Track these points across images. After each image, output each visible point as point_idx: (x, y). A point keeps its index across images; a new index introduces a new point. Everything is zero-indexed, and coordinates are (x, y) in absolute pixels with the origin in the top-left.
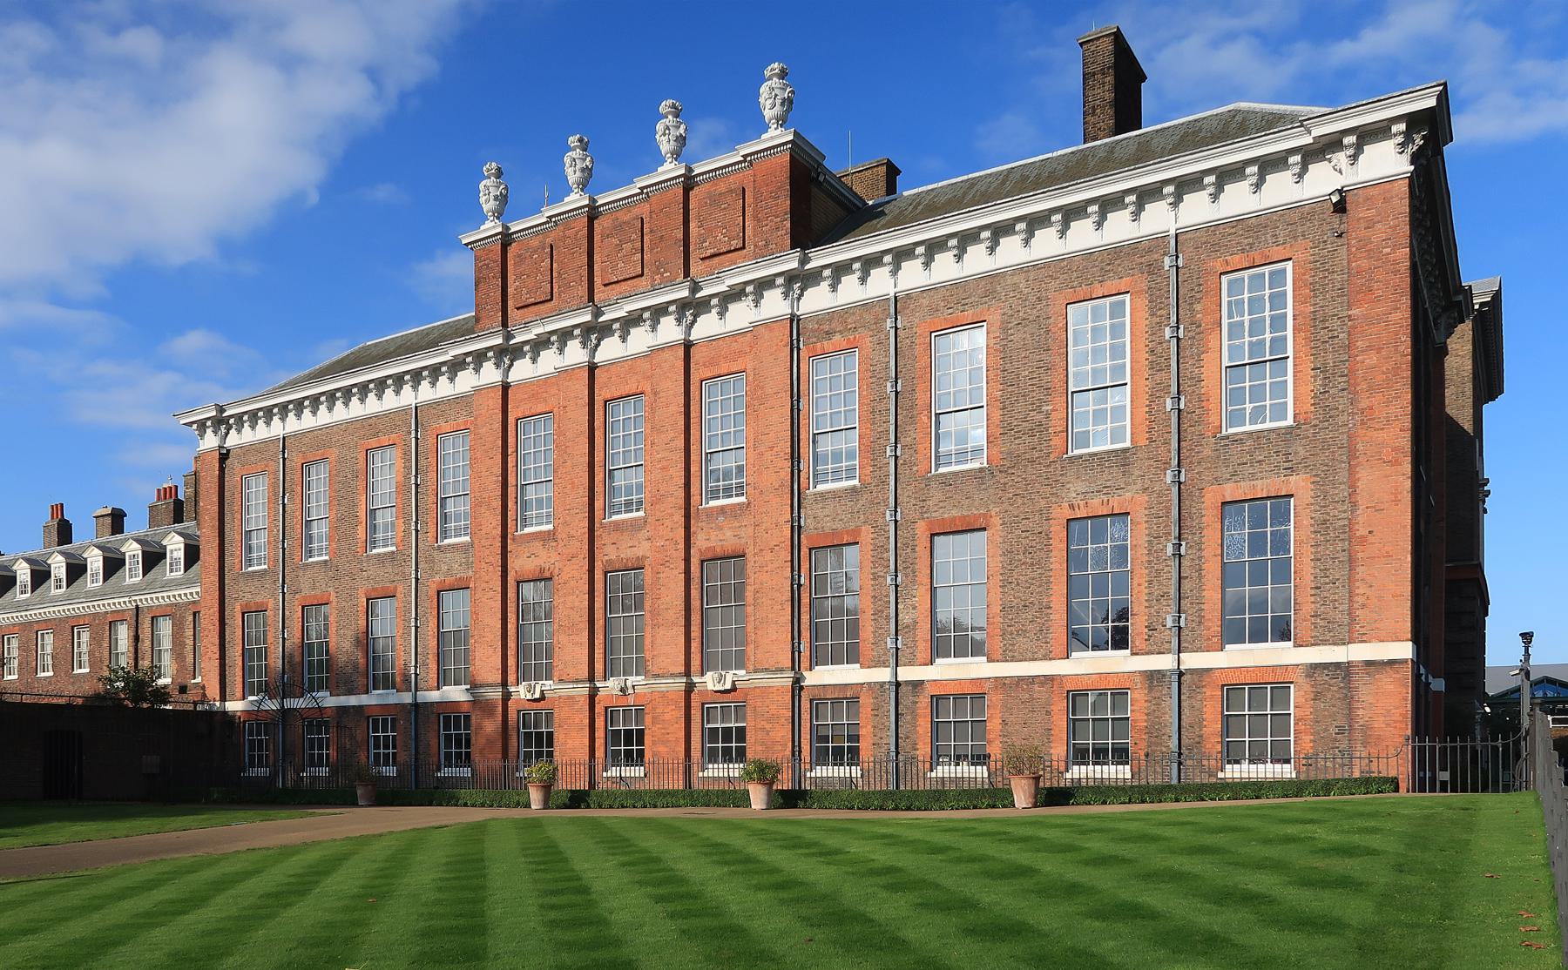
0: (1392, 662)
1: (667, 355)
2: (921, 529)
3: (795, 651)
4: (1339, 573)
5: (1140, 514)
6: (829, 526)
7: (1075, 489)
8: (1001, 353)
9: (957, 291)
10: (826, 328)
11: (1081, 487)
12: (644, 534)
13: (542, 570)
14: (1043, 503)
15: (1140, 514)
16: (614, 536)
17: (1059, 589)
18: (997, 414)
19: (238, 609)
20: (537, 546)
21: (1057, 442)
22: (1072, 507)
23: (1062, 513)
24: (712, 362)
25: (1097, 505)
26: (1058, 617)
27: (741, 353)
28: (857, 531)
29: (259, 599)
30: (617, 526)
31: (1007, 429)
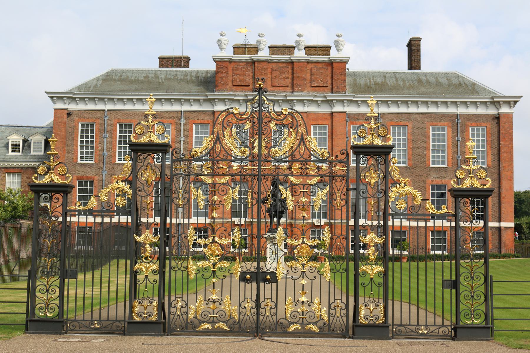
0: (510, 227)
4: (497, 205)
7: (433, 176)
8: (413, 135)
9: (399, 115)
10: (357, 117)
11: (435, 176)
14: (424, 179)
18: (411, 152)
21: (427, 162)
22: (432, 181)
23: (429, 182)
24: (316, 120)
25: (438, 181)
27: (326, 119)
29: (89, 175)
31: (414, 157)
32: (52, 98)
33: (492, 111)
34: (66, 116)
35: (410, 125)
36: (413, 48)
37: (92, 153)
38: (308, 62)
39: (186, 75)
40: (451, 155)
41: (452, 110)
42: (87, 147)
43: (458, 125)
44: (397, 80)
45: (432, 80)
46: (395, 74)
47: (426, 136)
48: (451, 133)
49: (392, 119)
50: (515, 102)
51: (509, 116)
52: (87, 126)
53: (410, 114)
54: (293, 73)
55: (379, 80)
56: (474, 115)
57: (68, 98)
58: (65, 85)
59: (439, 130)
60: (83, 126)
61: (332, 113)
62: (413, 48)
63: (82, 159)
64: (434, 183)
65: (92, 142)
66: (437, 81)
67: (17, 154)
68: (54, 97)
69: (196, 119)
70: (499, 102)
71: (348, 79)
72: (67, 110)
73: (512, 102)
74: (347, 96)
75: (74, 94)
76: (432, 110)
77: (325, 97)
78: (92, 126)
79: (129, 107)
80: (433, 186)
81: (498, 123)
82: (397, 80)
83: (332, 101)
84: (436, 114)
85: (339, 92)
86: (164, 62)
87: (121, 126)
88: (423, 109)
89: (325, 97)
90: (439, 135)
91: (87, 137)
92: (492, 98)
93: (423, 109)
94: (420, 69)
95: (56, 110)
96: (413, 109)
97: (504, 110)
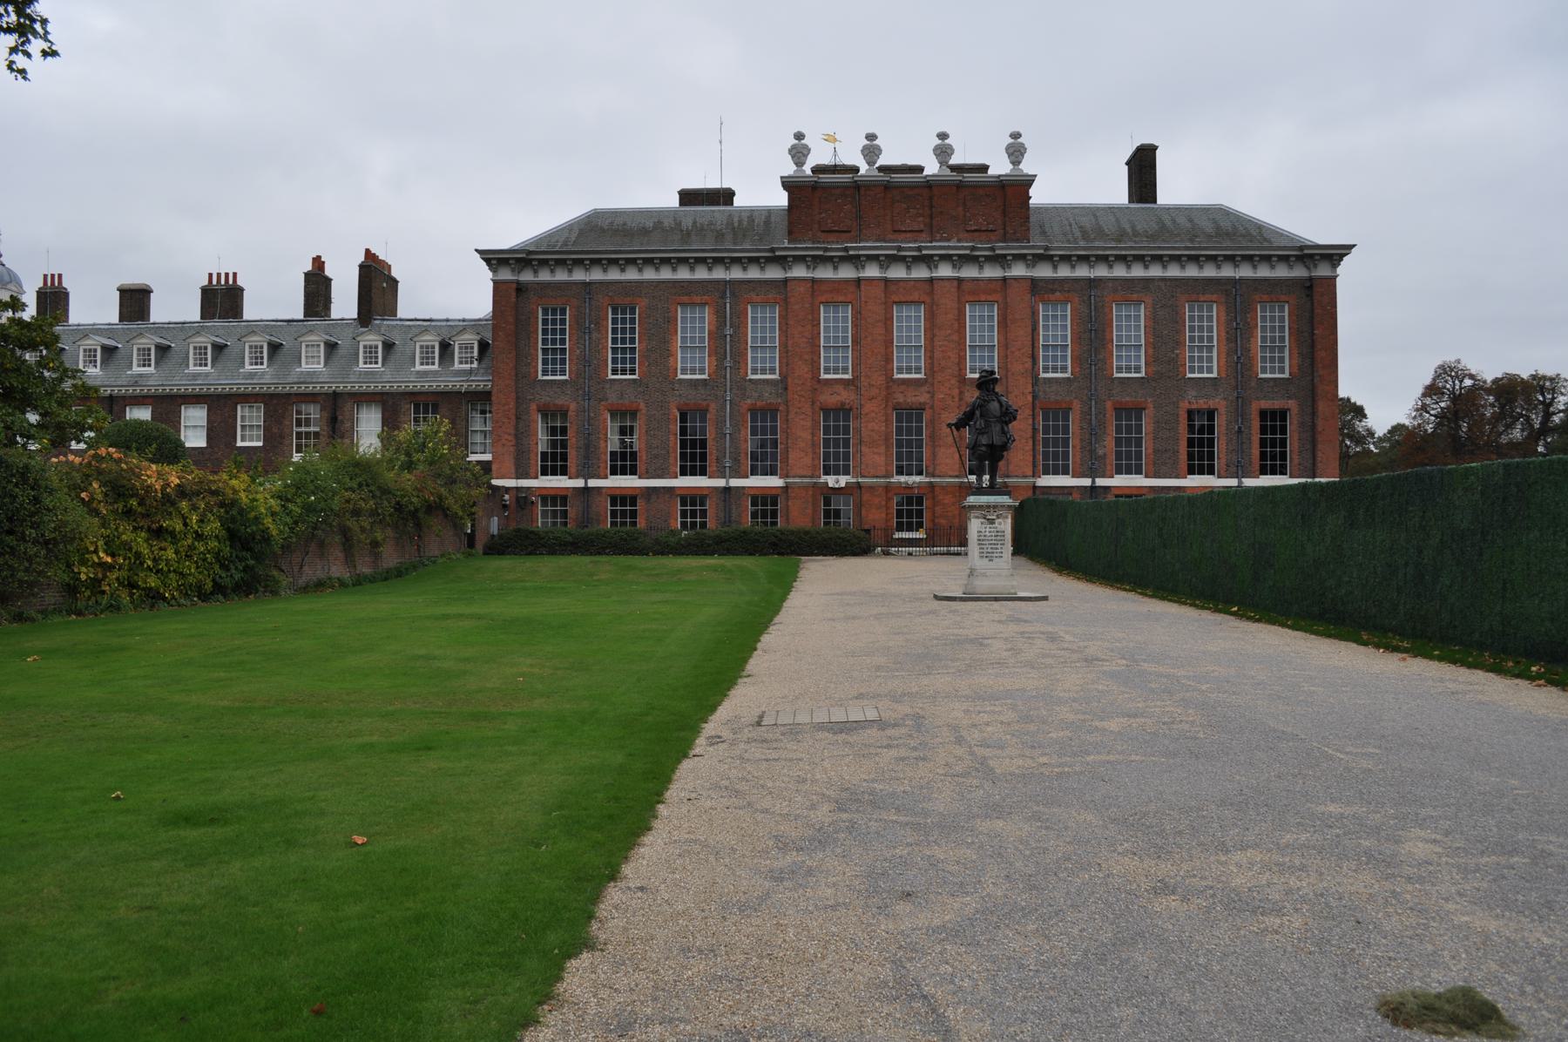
1: (946, 284)
2: (1109, 405)
3: (1034, 466)
5: (1223, 410)
6: (1053, 398)
12: (926, 388)
13: (843, 404)
15: (1223, 410)
16: (903, 387)
17: (1183, 444)
18: (1151, 351)
19: (534, 407)
20: (839, 388)
23: (1184, 405)
25: (1202, 404)
26: (1183, 456)
28: (1071, 402)
29: (559, 402)
30: (904, 381)
32: (488, 261)
33: (1299, 272)
34: (514, 294)
35: (1149, 301)
36: (1143, 166)
37: (563, 361)
38: (959, 186)
39: (730, 216)
40: (1223, 355)
41: (1227, 272)
42: (554, 350)
43: (1238, 301)
44: (1117, 220)
45: (1182, 220)
46: (1111, 210)
47: (1177, 321)
48: (1223, 314)
49: (1115, 290)
50: (1342, 256)
51: (1331, 282)
52: (554, 312)
53: (1147, 281)
54: (931, 207)
55: (1087, 222)
56: (1266, 280)
57: (518, 260)
58: (514, 233)
59: (1200, 309)
60: (545, 312)
61: (1004, 279)
62: (1143, 166)
63: (545, 372)
64: (1194, 406)
65: (563, 341)
66: (1191, 221)
67: (430, 367)
68: (494, 259)
69: (753, 295)
70: (1311, 256)
71: (1032, 219)
72: (518, 282)
73: (1335, 255)
74: (1033, 247)
75: (530, 252)
76: (1192, 272)
77: (992, 249)
78: (563, 312)
79: (631, 275)
80: (1190, 413)
81: (1310, 296)
82: (1117, 220)
83: (1005, 256)
84: (1196, 280)
85: (1017, 240)
86: (688, 197)
87: (615, 311)
88: (1174, 271)
89: (992, 249)
90: (1201, 318)
91: (554, 331)
92: (1301, 248)
93: (1174, 271)
94: (1155, 201)
95: (497, 285)
96: (1155, 271)
97: (1322, 271)
